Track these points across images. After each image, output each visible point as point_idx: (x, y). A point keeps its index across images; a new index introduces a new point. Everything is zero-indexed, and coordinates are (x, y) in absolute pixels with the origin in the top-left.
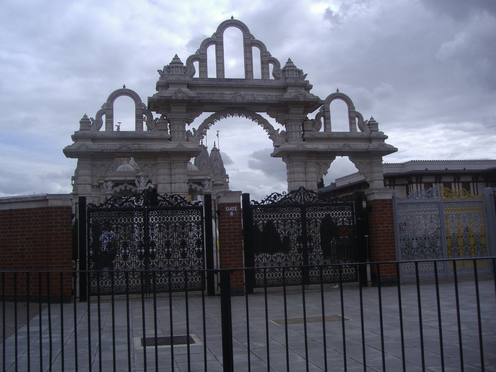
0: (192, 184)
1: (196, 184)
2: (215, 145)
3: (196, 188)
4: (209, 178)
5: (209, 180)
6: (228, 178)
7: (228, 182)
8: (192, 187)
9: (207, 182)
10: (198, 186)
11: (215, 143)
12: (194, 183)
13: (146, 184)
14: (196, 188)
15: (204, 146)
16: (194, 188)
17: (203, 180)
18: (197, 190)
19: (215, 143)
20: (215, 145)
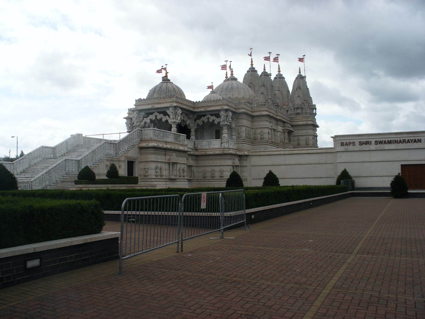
0: (209, 116)
1: (214, 117)
2: (300, 72)
3: (213, 121)
4: (226, 107)
5: (226, 110)
6: (316, 109)
7: (316, 114)
8: (210, 120)
9: (222, 113)
10: (216, 118)
11: (300, 70)
12: (212, 115)
13: (142, 119)
14: (213, 121)
15: (267, 73)
16: (211, 121)
17: (219, 110)
18: (215, 122)
19: (300, 70)
20: (300, 72)
